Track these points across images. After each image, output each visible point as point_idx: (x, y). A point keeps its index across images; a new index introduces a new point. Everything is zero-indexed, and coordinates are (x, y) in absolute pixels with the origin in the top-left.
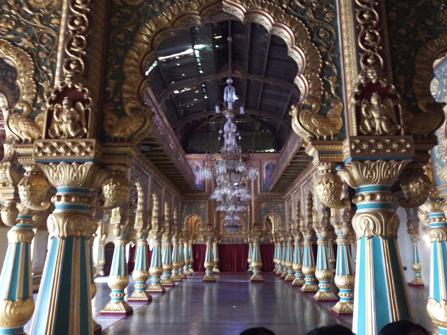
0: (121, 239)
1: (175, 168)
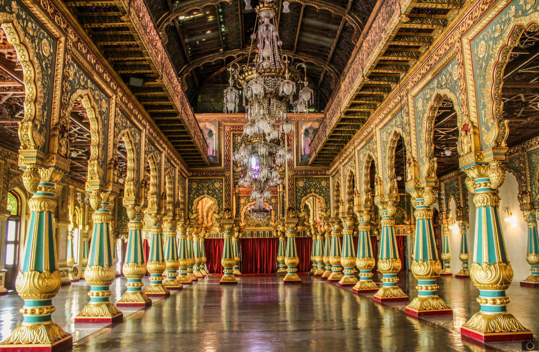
0: (102, 214)
1: (179, 121)
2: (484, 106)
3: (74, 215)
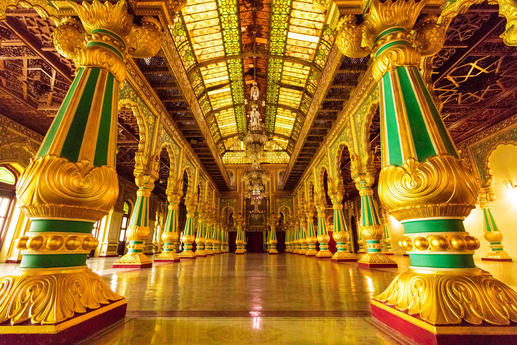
2: (361, 145)
3: (159, 217)
